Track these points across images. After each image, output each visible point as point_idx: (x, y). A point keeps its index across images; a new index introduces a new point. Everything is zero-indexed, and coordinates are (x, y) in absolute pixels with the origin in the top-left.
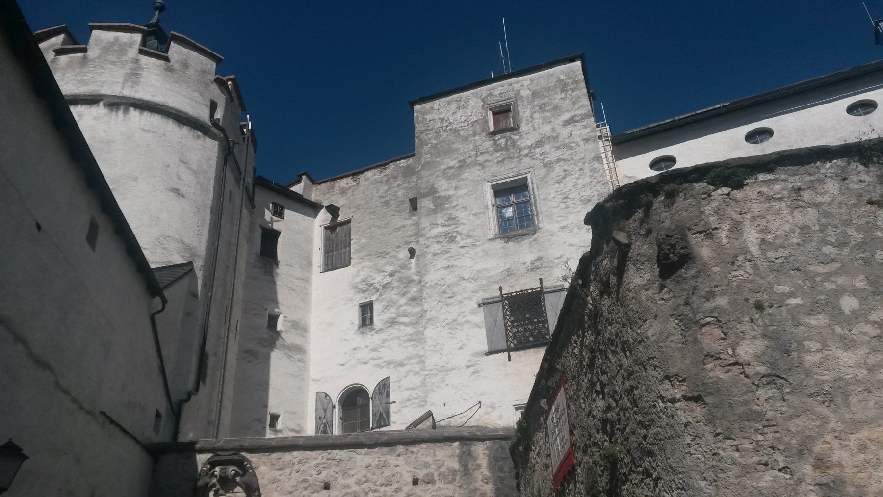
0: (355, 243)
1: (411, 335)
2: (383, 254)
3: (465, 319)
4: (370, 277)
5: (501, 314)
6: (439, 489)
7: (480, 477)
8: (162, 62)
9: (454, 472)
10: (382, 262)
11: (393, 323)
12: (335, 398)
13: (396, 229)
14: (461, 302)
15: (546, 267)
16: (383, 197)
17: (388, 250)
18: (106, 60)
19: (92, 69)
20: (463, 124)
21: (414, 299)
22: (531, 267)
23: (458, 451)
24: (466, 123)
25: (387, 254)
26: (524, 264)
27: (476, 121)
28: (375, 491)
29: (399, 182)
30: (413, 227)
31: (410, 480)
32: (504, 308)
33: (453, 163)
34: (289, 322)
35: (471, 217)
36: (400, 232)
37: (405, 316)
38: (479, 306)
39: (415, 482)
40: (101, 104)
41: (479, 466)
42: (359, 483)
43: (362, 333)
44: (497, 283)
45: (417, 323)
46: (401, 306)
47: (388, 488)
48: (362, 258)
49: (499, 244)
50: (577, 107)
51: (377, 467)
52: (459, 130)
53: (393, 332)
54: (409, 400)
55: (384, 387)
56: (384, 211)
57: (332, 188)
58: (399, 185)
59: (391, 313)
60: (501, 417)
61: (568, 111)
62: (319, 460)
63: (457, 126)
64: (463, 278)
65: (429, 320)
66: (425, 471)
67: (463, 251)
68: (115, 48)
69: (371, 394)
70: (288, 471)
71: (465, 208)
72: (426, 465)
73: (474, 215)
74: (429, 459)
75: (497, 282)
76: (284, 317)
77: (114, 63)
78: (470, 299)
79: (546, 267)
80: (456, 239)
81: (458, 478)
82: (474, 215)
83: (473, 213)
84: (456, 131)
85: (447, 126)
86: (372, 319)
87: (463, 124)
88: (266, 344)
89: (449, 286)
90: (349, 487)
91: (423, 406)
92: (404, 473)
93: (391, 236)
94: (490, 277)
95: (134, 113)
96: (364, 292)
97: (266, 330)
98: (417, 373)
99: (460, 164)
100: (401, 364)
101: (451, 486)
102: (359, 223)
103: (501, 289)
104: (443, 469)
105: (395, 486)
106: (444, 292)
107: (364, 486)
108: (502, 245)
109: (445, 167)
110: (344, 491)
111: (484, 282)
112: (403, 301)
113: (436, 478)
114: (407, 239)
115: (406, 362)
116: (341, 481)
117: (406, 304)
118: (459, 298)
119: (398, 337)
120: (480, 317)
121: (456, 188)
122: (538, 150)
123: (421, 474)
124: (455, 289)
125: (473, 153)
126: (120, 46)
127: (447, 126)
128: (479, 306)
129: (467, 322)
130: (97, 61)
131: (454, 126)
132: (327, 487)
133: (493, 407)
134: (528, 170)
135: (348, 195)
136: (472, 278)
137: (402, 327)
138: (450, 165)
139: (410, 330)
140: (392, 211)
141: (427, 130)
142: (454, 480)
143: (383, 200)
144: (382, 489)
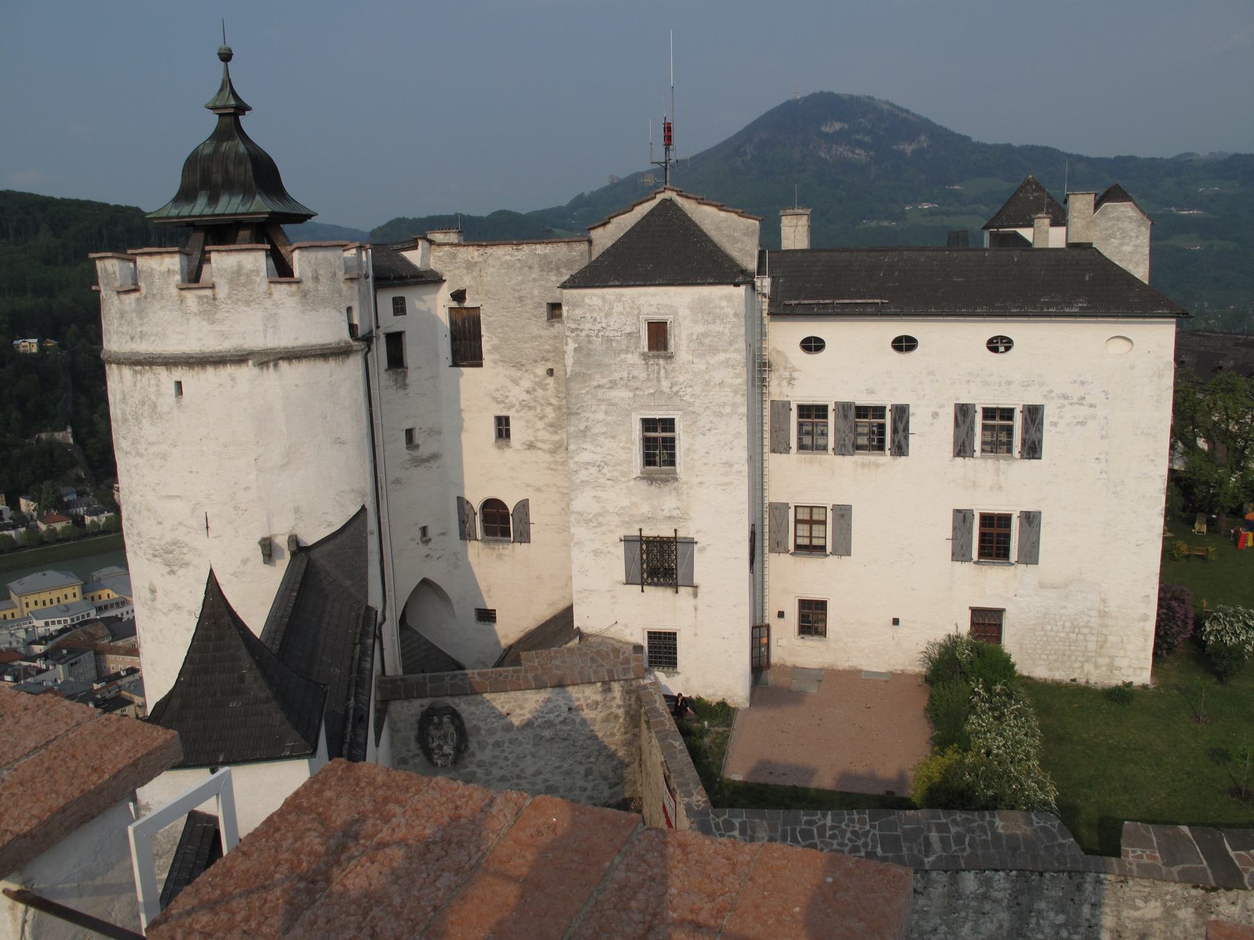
0: (487, 341)
1: (549, 463)
2: (519, 365)
3: (608, 550)
4: (505, 387)
5: (638, 552)
7: (615, 705)
8: (294, 287)
9: (597, 703)
10: (519, 374)
11: (531, 446)
12: (477, 504)
13: (533, 337)
14: (604, 533)
15: (681, 518)
16: (515, 290)
17: (524, 362)
18: (238, 300)
19: (227, 315)
20: (616, 334)
21: (551, 425)
22: (668, 514)
23: (600, 689)
24: (619, 334)
25: (523, 365)
26: (663, 510)
27: (629, 333)
28: (543, 717)
29: (534, 276)
30: (551, 342)
31: (567, 709)
32: (641, 548)
33: (604, 381)
34: (425, 432)
35: (619, 450)
36: (537, 343)
37: (544, 442)
38: (621, 540)
40: (250, 362)
41: (614, 698)
43: (499, 448)
44: (638, 523)
45: (555, 452)
46: (538, 430)
47: (551, 715)
48: (495, 363)
49: (643, 485)
50: (733, 348)
52: (611, 340)
53: (530, 455)
54: (547, 525)
55: (523, 506)
56: (518, 309)
57: (454, 256)
58: (534, 280)
59: (528, 436)
60: (631, 634)
61: (725, 351)
62: (502, 699)
63: (611, 335)
64: (608, 511)
65: (576, 543)
67: (609, 482)
68: (243, 279)
69: (511, 512)
70: (481, 707)
71: (613, 437)
73: (622, 448)
74: (580, 695)
75: (638, 523)
76: (420, 429)
77: (247, 303)
78: (611, 531)
79: (681, 518)
80: (603, 471)
81: (599, 707)
82: (622, 448)
83: (621, 445)
84: (609, 340)
85: (599, 331)
86: (508, 431)
87: (616, 334)
88: (408, 466)
89: (595, 516)
90: (523, 715)
91: (560, 533)
92: (562, 705)
93: (527, 345)
94: (632, 516)
95: (284, 365)
96: (499, 403)
97: (406, 451)
98: (555, 502)
99: (611, 385)
100: (538, 490)
101: (595, 712)
102: (490, 317)
103: (641, 530)
104: (589, 701)
105: (557, 713)
106: (591, 520)
108: (645, 487)
109: (595, 383)
110: (521, 718)
111: (627, 519)
112: (540, 425)
113: (584, 707)
114: (545, 354)
115: (543, 489)
116: (518, 711)
117: (544, 429)
118: (604, 529)
119: (536, 462)
120: (620, 550)
121: (606, 413)
122: (689, 390)
124: (600, 519)
125: (625, 375)
126: (248, 276)
127: (599, 331)
128: (621, 540)
129: (609, 552)
130: (229, 302)
131: (607, 333)
133: (626, 626)
134: (677, 412)
135: (475, 273)
136: (617, 513)
137: (540, 452)
138: (600, 383)
139: (548, 458)
140: (527, 312)
141: (577, 329)
142: (597, 708)
143: (517, 295)
144: (547, 716)
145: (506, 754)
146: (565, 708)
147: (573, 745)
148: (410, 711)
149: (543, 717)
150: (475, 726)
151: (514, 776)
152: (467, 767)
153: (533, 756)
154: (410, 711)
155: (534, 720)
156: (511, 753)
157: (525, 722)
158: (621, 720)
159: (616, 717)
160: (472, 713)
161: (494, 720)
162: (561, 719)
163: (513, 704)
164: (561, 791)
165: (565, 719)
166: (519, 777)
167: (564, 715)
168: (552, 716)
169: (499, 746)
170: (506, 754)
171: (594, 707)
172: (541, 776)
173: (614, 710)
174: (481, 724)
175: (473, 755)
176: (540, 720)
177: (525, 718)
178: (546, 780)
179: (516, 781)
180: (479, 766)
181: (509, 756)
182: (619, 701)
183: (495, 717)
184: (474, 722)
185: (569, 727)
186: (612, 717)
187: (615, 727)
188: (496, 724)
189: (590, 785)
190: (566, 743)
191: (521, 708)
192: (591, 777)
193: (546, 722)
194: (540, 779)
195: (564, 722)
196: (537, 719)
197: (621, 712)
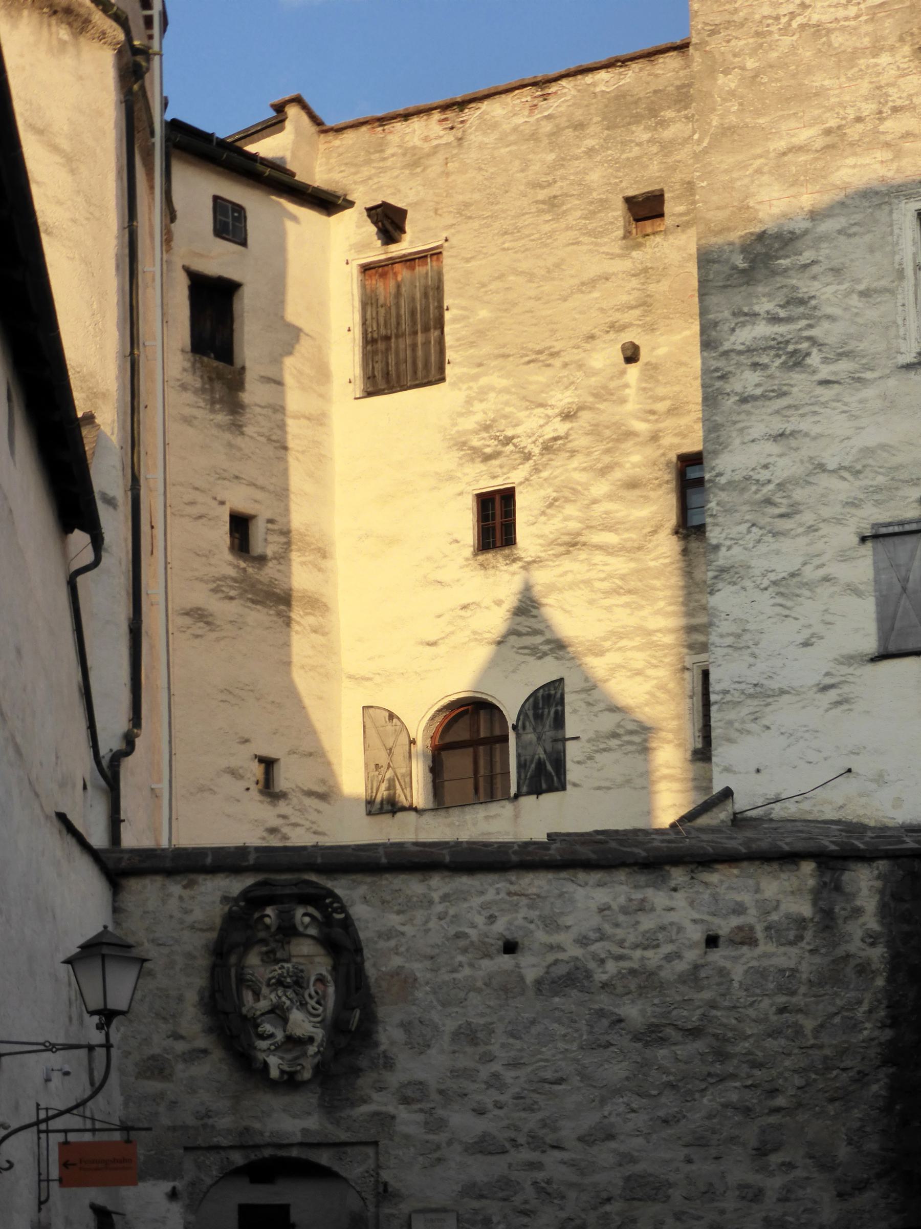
6: (766, 955)
7: (859, 933)
9: (801, 923)
23: (811, 882)
28: (620, 958)
39: (712, 941)
41: (858, 912)
42: (583, 941)
47: (649, 953)
51: (624, 911)
62: (490, 895)
66: (735, 921)
70: (419, 915)
72: (739, 909)
74: (746, 898)
90: (560, 948)
101: (793, 951)
104: (774, 917)
105: (667, 949)
107: (596, 947)
110: (550, 958)
113: (760, 934)
123: (725, 926)
132: (510, 948)
142: (800, 938)
144: (638, 953)
145: (496, 1067)
146: (696, 934)
147: (721, 1055)
148: (187, 912)
149: (620, 958)
150: (397, 972)
151: (522, 1140)
152: (365, 1101)
153: (584, 1076)
154: (187, 912)
155: (592, 965)
156: (514, 1064)
157: (562, 970)
158: (880, 982)
159: (863, 969)
160: (389, 934)
161: (460, 958)
162: (681, 966)
163: (523, 912)
164: (677, 1195)
165: (696, 967)
166: (536, 1143)
167: (691, 956)
168: (653, 957)
169: (473, 1040)
170: (496, 1067)
171: (791, 935)
172: (613, 1145)
173: (855, 946)
174: (417, 967)
175: (389, 1063)
176: (611, 967)
177: (561, 956)
178: (628, 1158)
179: (526, 1155)
180: (406, 1101)
181: (509, 1076)
182: (871, 922)
183: (465, 951)
184: (397, 961)
185: (707, 995)
186: (849, 971)
187: (860, 1002)
188: (467, 971)
189: (774, 1184)
190: (700, 1045)
191: (551, 923)
192: (775, 1159)
193: (633, 972)
194: (604, 1154)
195: (693, 977)
196: (602, 961)
197: (877, 954)
